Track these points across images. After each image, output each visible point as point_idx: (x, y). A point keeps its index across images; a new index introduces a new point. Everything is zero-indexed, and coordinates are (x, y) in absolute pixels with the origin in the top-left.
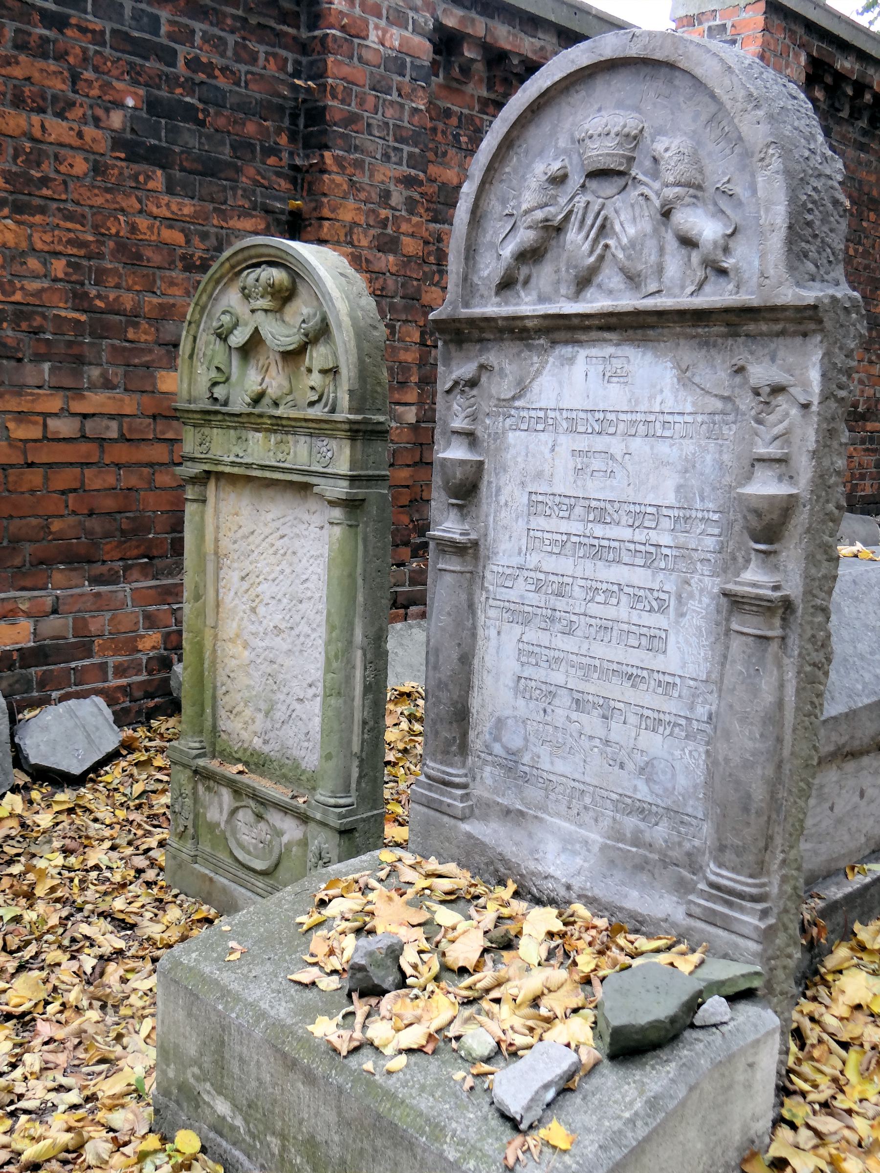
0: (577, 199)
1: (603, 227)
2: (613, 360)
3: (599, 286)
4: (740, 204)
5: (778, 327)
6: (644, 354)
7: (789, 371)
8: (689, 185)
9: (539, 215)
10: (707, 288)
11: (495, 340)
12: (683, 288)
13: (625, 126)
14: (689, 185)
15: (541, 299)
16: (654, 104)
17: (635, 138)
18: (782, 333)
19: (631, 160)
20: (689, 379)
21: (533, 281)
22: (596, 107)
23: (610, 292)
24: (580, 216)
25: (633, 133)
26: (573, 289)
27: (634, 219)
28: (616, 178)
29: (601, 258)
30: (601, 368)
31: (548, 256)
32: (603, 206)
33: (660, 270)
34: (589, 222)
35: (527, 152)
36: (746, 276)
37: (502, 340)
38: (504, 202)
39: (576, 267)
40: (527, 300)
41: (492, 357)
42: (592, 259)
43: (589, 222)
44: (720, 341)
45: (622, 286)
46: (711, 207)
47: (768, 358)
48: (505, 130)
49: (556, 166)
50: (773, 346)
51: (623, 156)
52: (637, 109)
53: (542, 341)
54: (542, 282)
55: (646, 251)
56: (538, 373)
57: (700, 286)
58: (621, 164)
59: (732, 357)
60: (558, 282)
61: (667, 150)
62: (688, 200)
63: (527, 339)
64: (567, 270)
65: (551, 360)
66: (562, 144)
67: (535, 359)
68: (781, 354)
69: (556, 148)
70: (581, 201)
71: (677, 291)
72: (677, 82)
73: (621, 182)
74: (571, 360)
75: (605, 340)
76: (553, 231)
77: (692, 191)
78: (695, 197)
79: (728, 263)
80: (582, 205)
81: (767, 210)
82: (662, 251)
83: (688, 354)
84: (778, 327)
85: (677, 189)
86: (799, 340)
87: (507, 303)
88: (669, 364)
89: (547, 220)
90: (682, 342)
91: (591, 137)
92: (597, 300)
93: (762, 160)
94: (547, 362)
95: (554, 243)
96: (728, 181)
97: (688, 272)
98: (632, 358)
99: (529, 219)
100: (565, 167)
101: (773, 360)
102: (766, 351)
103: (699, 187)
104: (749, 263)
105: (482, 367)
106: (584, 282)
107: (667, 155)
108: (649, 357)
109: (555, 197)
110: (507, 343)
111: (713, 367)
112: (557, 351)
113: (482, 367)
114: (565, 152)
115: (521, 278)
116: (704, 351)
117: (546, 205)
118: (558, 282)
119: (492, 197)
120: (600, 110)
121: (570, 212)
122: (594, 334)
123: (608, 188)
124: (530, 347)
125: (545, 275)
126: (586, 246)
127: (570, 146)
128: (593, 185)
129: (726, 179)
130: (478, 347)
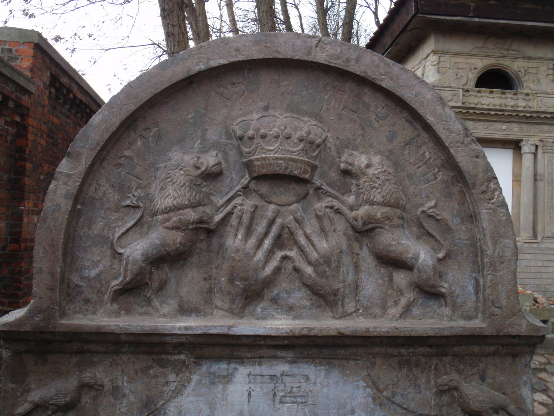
0: (238, 200)
1: (279, 237)
2: (287, 379)
3: (275, 301)
4: (446, 229)
5: (492, 349)
6: (328, 373)
7: (500, 389)
8: (395, 205)
9: (191, 215)
10: (415, 311)
11: (105, 353)
12: (384, 308)
13: (309, 133)
14: (395, 205)
15: (184, 310)
16: (340, 116)
17: (318, 146)
18: (493, 354)
19: (314, 168)
20: (388, 399)
21: (172, 287)
22: (261, 104)
23: (290, 308)
24: (246, 219)
25: (318, 141)
26: (239, 303)
27: (323, 230)
28: (293, 185)
29: (278, 270)
30: (272, 386)
31: (194, 259)
32: (277, 214)
33: (356, 287)
34: (260, 228)
35: (159, 137)
36: (460, 300)
37: (117, 353)
38: (123, 189)
39: (244, 279)
40: (166, 309)
41: (99, 373)
42: (269, 270)
43: (260, 228)
44: (423, 360)
45: (307, 303)
46: (414, 229)
47: (477, 377)
48: (133, 108)
49: (210, 160)
50: (482, 366)
51: (308, 164)
52: (316, 116)
53: (183, 357)
54: (184, 291)
55: (343, 269)
56: (178, 392)
57: (407, 309)
58: (305, 172)
59: (437, 376)
60: (210, 291)
61: (368, 166)
62: (396, 221)
63: (160, 353)
64: (231, 281)
65: (195, 377)
66: (213, 135)
67: (172, 377)
68: (490, 373)
69: (203, 139)
70: (247, 204)
71: (377, 311)
72: (366, 99)
73: (301, 189)
74: (228, 379)
75: (275, 357)
76: (206, 232)
77: (399, 212)
78: (402, 218)
79: (444, 288)
80: (250, 209)
81: (495, 242)
82: (357, 267)
83: (386, 374)
84: (492, 349)
85: (385, 209)
86: (509, 360)
87: (128, 311)
88: (362, 384)
89: (201, 222)
90: (379, 361)
91: (263, 137)
92: (273, 317)
93: (484, 192)
94: (189, 380)
95: (202, 246)
96: (435, 206)
97: (390, 292)
98: (312, 377)
99: (175, 219)
100: (219, 164)
101: (483, 379)
102: (475, 370)
103: (404, 209)
104: (463, 288)
105: (84, 386)
106: (252, 293)
107: (371, 171)
108: (335, 374)
109: (208, 195)
110: (125, 358)
111: (417, 386)
112: (204, 368)
113: (84, 386)
114: (216, 146)
115: (156, 284)
116: (405, 371)
117: (200, 204)
118: (210, 291)
119: (103, 181)
120: (266, 109)
121: (230, 214)
122: (263, 352)
123: (286, 194)
124: (162, 364)
125: (189, 282)
126: (260, 255)
127: (223, 140)
128: (264, 188)
129: (432, 203)
130: (74, 360)
